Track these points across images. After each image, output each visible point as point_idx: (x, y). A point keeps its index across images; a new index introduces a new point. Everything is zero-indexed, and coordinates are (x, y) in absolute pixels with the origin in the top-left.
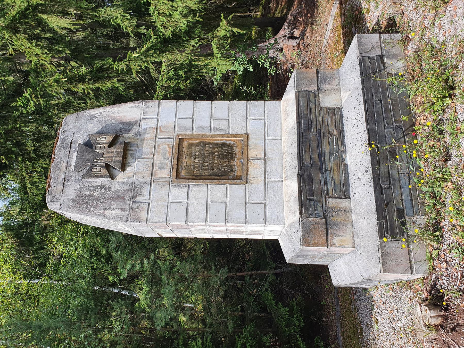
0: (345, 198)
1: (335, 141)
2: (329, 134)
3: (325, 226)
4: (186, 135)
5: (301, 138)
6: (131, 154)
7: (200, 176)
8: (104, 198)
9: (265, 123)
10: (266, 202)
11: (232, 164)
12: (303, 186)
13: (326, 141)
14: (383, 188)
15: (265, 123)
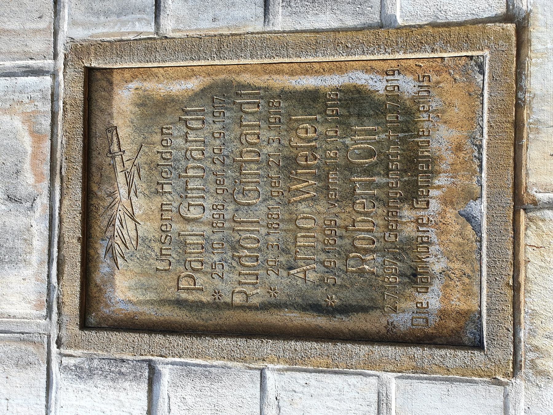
4: (121, 47)
7: (217, 306)
11: (409, 230)
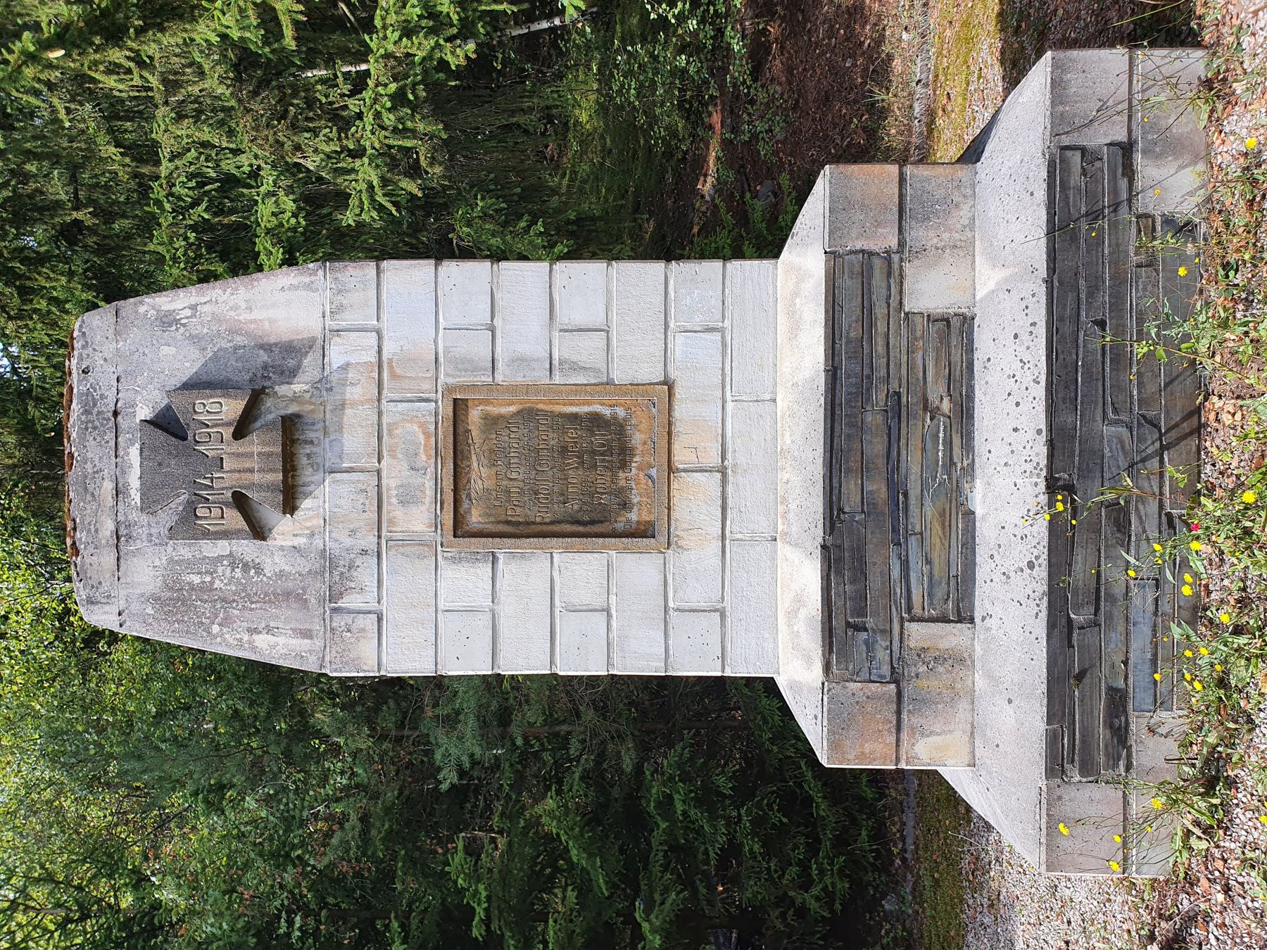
0: (959, 621)
1: (941, 435)
2: (925, 408)
3: (895, 706)
4: (473, 387)
5: (837, 425)
6: (309, 456)
7: (527, 523)
8: (247, 596)
9: (724, 344)
10: (727, 604)
11: (622, 483)
12: (837, 584)
13: (915, 431)
14: (1075, 625)
15: (724, 344)
